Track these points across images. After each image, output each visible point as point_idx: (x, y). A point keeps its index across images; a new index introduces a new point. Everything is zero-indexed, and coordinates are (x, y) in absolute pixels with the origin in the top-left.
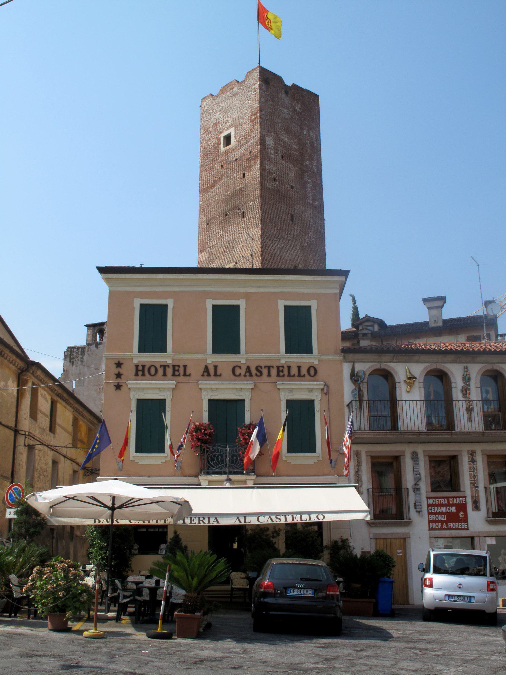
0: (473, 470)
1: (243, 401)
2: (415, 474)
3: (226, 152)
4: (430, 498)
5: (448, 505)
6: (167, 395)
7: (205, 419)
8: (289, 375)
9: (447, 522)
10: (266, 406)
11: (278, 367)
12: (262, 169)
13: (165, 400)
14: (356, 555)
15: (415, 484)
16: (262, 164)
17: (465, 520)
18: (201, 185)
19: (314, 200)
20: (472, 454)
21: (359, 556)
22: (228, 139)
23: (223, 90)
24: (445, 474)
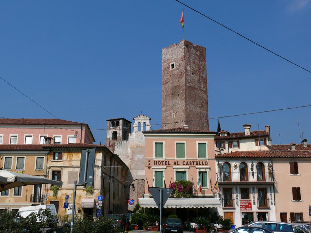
3: (172, 71)
5: (246, 203)
8: (199, 164)
11: (196, 162)
12: (186, 79)
16: (185, 77)
17: (251, 207)
19: (204, 88)
22: (173, 65)
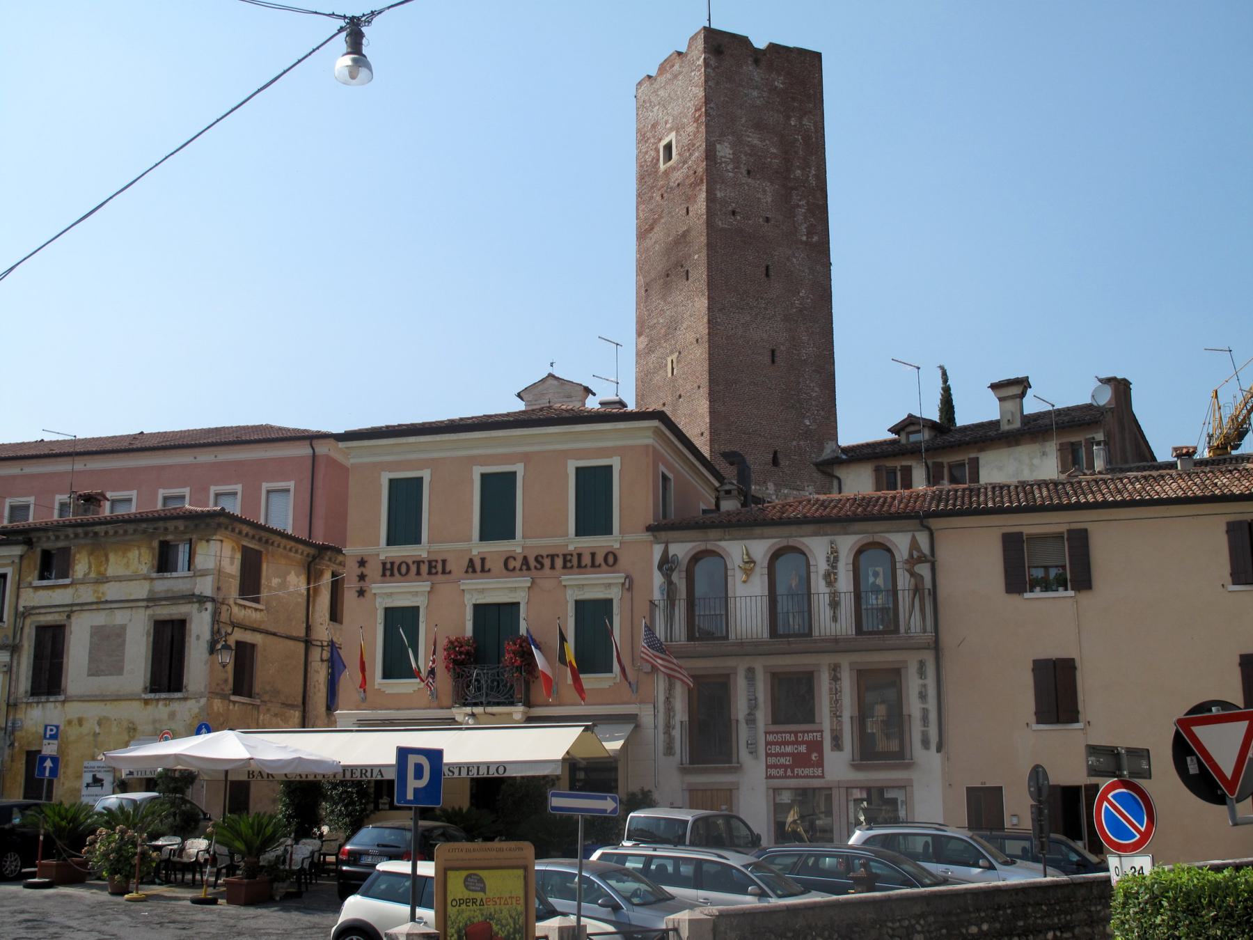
0: (836, 693)
1: (518, 604)
2: (749, 700)
3: (666, 173)
4: (769, 733)
5: (796, 743)
6: (420, 601)
7: (469, 632)
8: (579, 566)
9: (792, 767)
10: (546, 612)
11: (565, 556)
13: (418, 608)
14: (460, 809)
15: (749, 714)
17: (820, 763)
18: (639, 227)
19: (810, 233)
20: (835, 669)
21: (465, 810)
22: (668, 148)
23: (662, 69)
24: (793, 699)
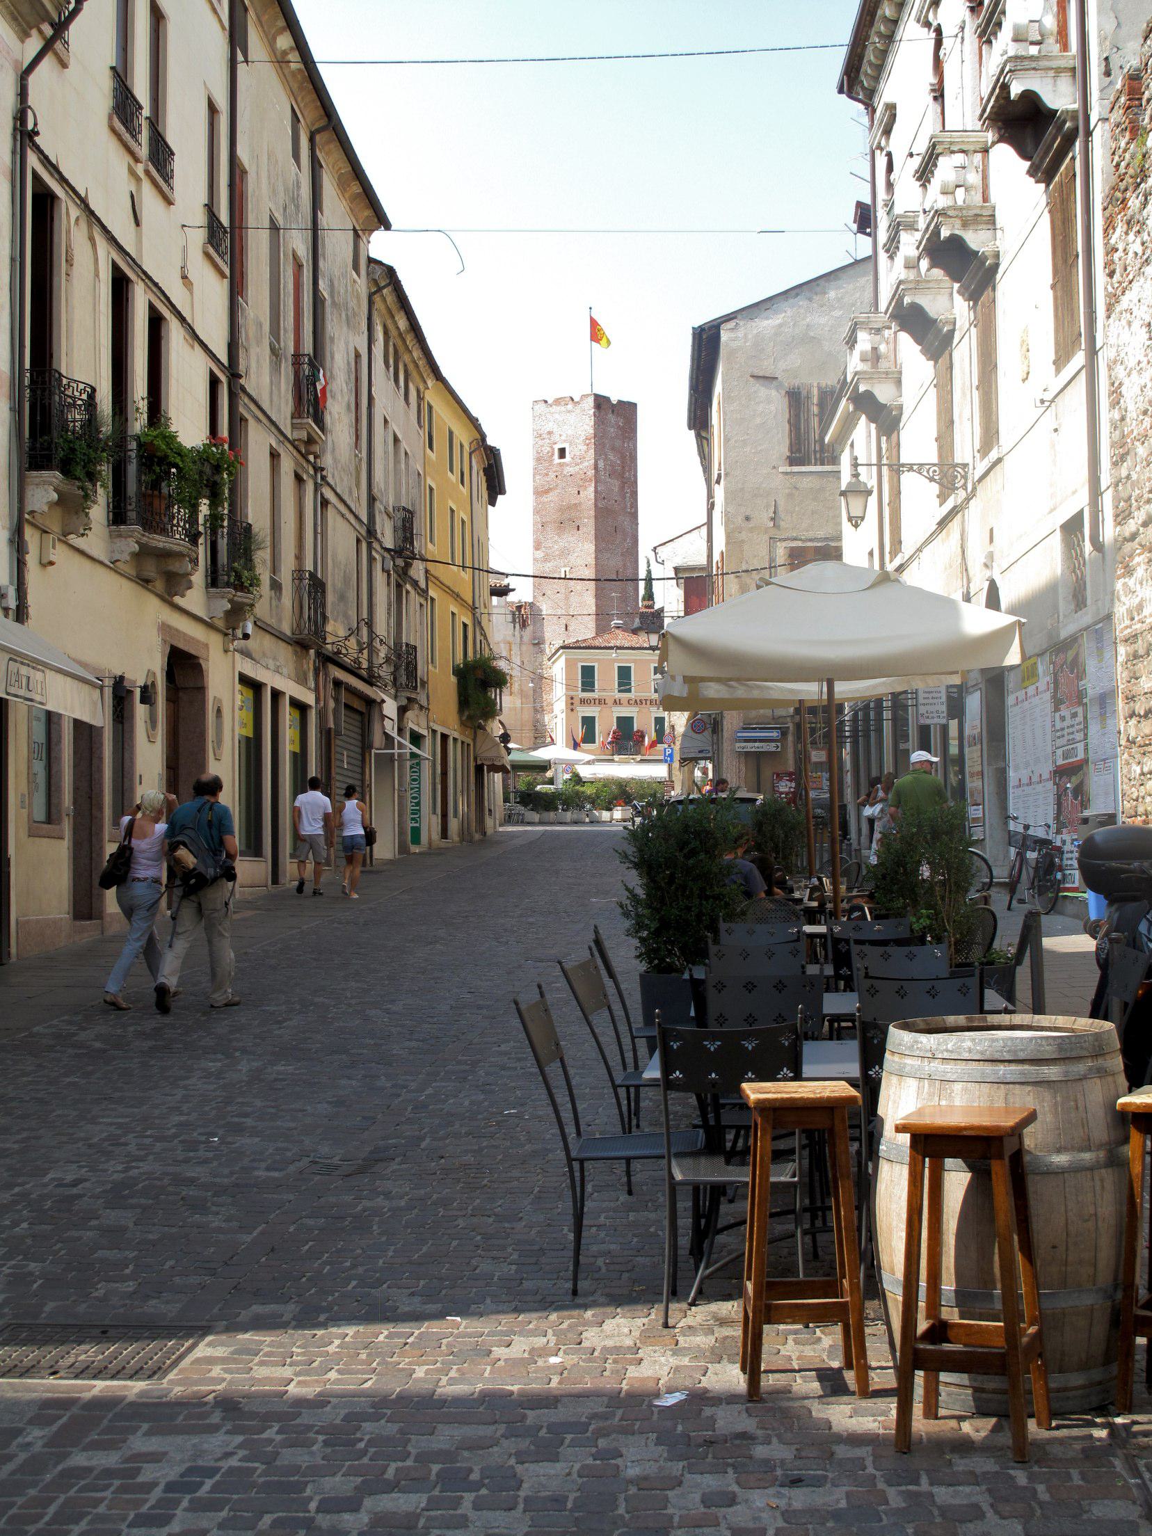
6: (596, 715)
10: (644, 720)
12: (596, 491)
16: (596, 487)
18: (535, 488)
22: (562, 453)
23: (558, 401)
